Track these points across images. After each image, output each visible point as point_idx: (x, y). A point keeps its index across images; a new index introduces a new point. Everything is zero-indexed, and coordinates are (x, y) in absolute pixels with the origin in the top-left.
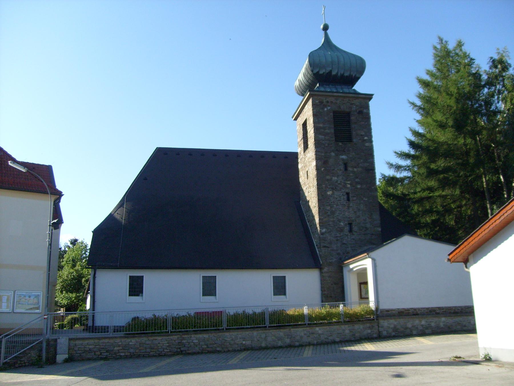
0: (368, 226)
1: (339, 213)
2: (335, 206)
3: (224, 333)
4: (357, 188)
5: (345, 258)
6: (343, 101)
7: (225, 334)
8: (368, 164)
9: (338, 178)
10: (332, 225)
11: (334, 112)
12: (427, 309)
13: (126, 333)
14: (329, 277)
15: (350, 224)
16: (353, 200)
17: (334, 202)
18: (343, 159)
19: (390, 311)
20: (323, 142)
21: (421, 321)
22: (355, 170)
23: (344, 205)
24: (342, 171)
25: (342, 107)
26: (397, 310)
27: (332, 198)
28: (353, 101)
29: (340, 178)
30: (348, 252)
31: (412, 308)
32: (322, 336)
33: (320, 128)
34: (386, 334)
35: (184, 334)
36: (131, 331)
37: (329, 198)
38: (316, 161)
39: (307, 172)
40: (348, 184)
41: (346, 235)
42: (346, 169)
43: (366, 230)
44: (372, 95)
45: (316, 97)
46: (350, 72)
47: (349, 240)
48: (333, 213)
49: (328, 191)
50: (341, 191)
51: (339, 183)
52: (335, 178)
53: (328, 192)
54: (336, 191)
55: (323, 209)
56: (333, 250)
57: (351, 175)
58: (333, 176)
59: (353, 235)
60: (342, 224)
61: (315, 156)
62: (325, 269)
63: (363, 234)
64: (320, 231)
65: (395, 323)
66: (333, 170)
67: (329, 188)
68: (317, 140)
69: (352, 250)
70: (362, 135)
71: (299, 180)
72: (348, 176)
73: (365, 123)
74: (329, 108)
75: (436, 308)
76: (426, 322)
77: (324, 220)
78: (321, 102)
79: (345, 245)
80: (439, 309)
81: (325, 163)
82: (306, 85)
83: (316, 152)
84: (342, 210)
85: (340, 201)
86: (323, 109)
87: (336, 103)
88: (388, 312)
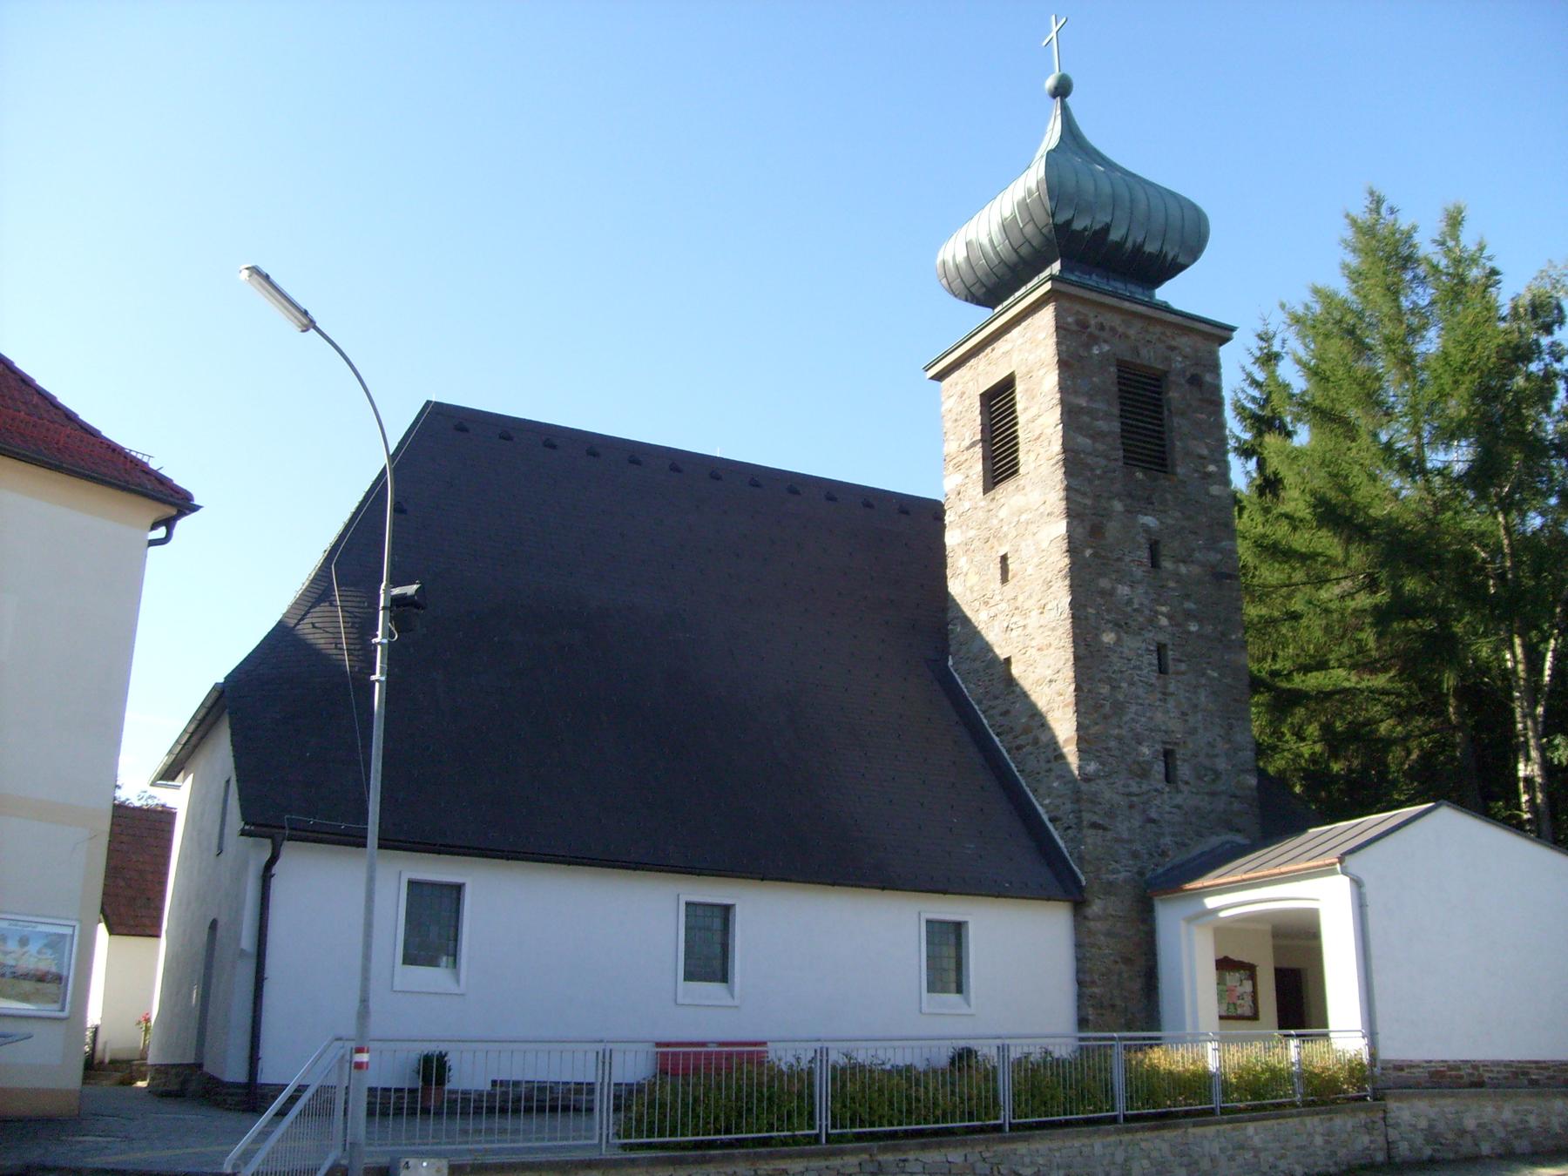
0: (1221, 764)
1: (1136, 713)
2: (1124, 685)
3: (1013, 1146)
4: (1190, 633)
5: (1154, 869)
6: (1147, 331)
7: (1016, 1150)
8: (1219, 557)
9: (1133, 591)
10: (1116, 753)
11: (1122, 366)
12: (1508, 1064)
13: (626, 1144)
14: (1109, 934)
15: (1168, 755)
16: (1178, 673)
17: (1121, 672)
18: (1146, 529)
19: (1406, 1071)
20: (1089, 460)
21: (1499, 1109)
22: (1183, 569)
23: (1152, 685)
24: (1144, 569)
25: (1144, 352)
26: (1425, 1065)
27: (1114, 658)
28: (1174, 338)
29: (1140, 590)
30: (1163, 852)
31: (1467, 1062)
32: (1262, 1155)
33: (1081, 410)
34: (1407, 1153)
35: (885, 1150)
36: (681, 1136)
37: (1108, 656)
38: (1068, 523)
39: (1004, 559)
40: (1162, 614)
41: (1156, 790)
42: (1155, 563)
43: (1214, 781)
44: (1232, 329)
45: (1067, 304)
46: (1163, 244)
47: (1167, 809)
48: (1119, 708)
49: (1104, 631)
50: (1140, 634)
51: (1136, 606)
52: (1123, 590)
53: (1104, 635)
54: (1126, 633)
55: (1089, 691)
56: (1118, 840)
57: (1172, 584)
58: (1119, 581)
59: (1179, 791)
60: (1146, 751)
61: (1065, 503)
62: (1096, 908)
63: (1207, 793)
64: (1080, 768)
65: (1432, 1112)
66: (1119, 559)
67: (1108, 621)
68: (1073, 451)
69: (1176, 843)
70: (1201, 457)
71: (946, 587)
72: (1162, 587)
73: (1210, 418)
74: (1106, 348)
75: (1530, 1062)
76: (1515, 1112)
77: (1093, 730)
78: (1083, 325)
79: (1153, 825)
80: (1537, 1068)
81: (1096, 531)
82: (1002, 261)
83: (1068, 489)
84: (1147, 701)
85: (1141, 669)
86: (1088, 347)
87: (1127, 337)
88: (1400, 1074)
